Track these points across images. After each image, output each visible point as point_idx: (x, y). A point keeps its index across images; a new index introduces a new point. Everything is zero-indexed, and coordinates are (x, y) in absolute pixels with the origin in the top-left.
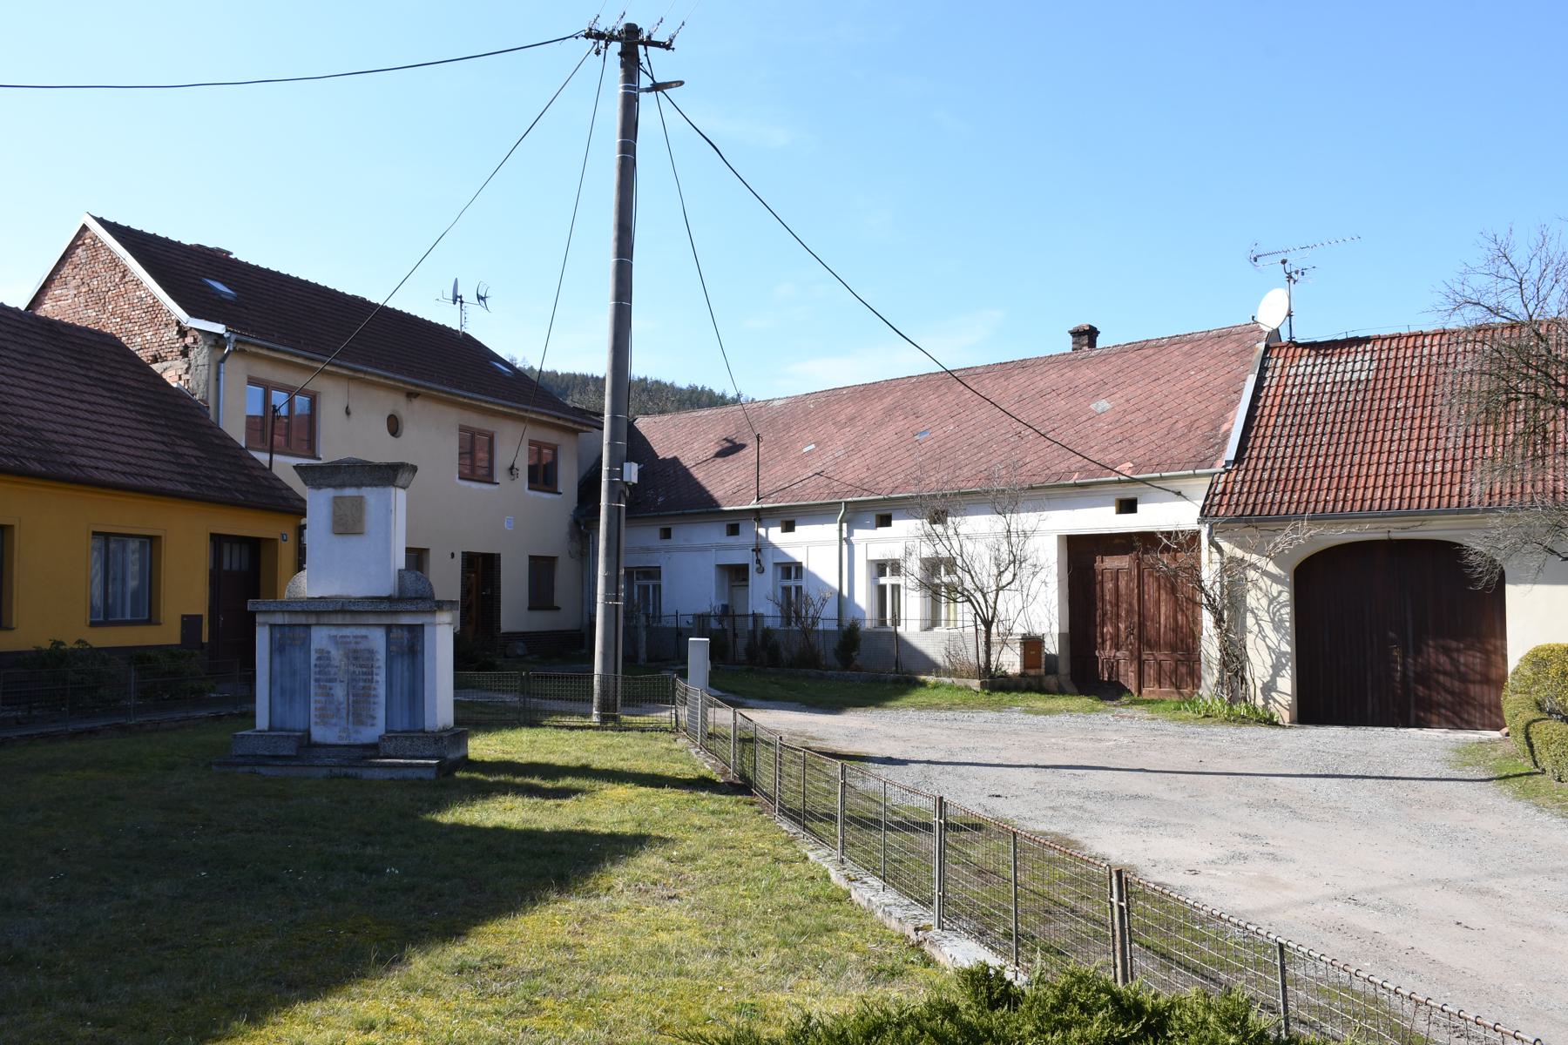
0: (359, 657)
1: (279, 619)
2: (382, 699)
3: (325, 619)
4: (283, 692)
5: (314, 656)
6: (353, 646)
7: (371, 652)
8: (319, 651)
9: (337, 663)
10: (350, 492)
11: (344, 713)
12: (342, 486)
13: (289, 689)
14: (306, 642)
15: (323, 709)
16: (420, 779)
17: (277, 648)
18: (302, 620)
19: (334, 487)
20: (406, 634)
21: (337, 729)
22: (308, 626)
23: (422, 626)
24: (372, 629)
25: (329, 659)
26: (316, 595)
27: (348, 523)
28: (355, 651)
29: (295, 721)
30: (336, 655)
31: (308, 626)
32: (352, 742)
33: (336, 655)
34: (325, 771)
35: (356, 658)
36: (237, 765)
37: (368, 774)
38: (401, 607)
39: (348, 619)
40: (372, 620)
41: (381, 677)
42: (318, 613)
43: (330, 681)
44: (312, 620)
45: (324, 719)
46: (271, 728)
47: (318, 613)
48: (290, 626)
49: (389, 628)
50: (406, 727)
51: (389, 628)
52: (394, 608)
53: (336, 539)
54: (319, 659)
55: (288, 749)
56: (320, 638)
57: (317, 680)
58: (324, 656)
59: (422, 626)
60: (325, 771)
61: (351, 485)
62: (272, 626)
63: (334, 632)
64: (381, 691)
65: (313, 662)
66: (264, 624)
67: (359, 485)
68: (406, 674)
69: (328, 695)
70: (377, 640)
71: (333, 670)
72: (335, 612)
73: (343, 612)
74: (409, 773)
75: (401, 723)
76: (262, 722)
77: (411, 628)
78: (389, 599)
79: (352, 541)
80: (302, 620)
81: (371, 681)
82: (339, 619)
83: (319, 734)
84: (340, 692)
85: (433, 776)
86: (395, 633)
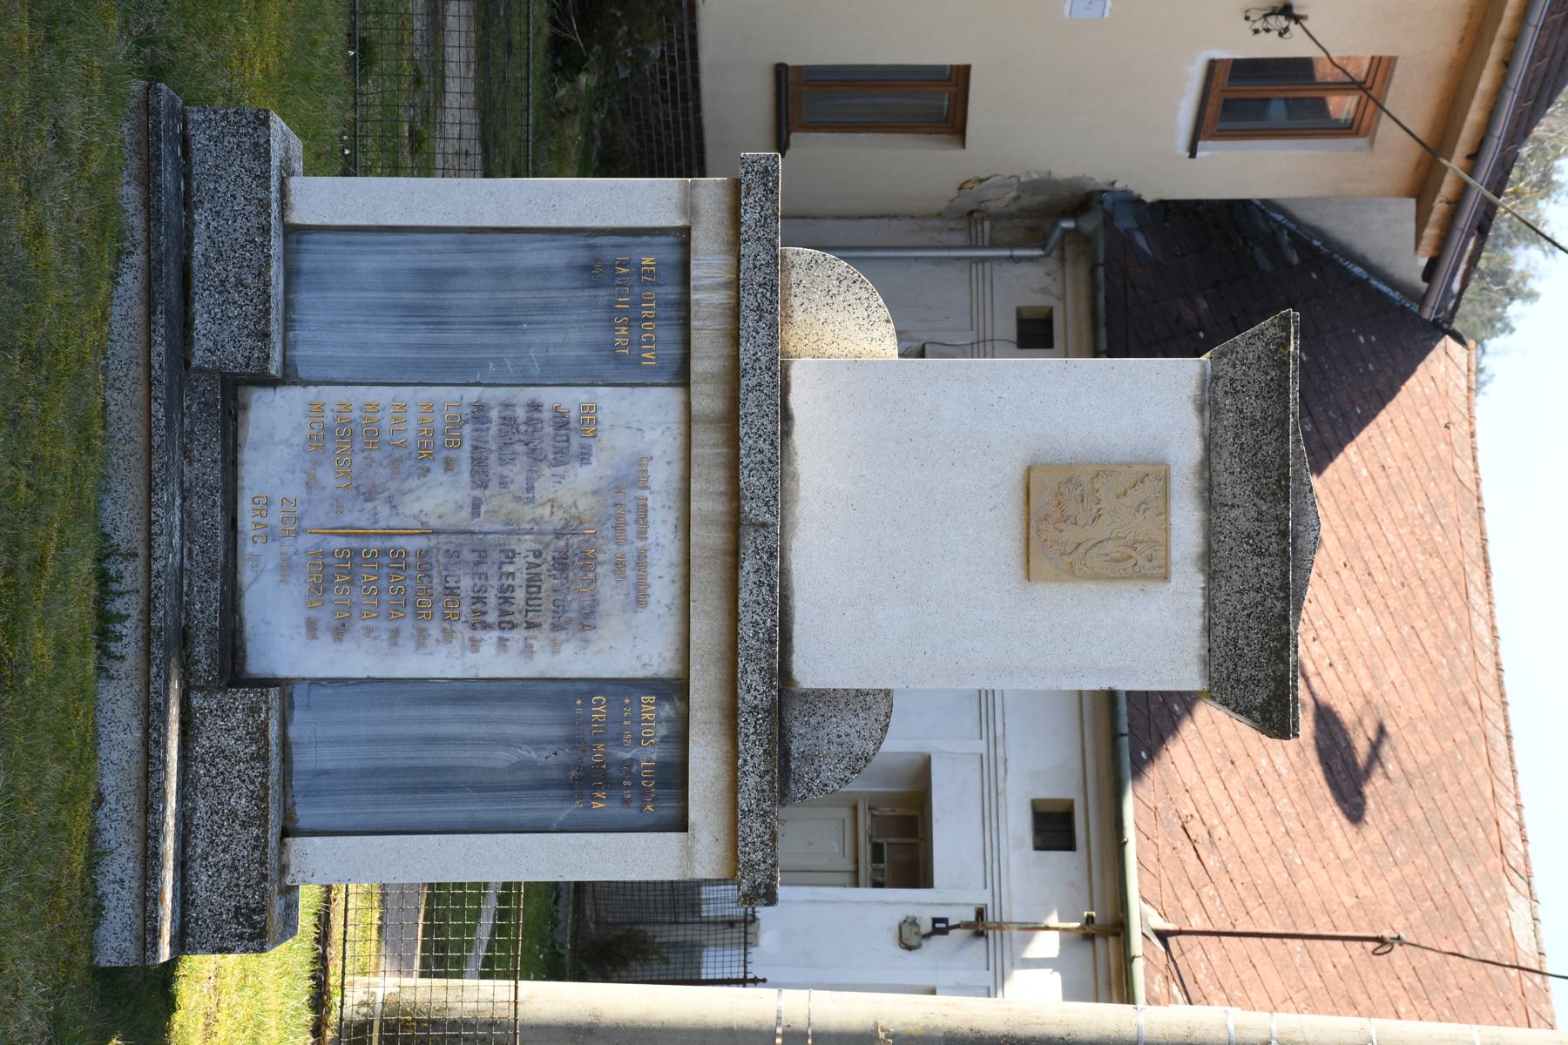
0: (564, 578)
1: (709, 265)
2: (410, 664)
3: (708, 446)
4: (434, 278)
5: (570, 399)
6: (608, 552)
7: (587, 621)
8: (589, 419)
9: (545, 486)
10: (1186, 525)
11: (357, 516)
12: (1210, 497)
13: (437, 285)
14: (621, 370)
15: (373, 437)
16: (98, 911)
17: (599, 259)
18: (707, 360)
19: (1206, 464)
20: (650, 755)
21: (295, 490)
22: (682, 377)
23: (681, 825)
24: (671, 624)
25: (561, 457)
26: (798, 400)
27: (1065, 519)
28: (588, 561)
29: (322, 330)
30: (574, 488)
31: (682, 377)
32: (248, 549)
33: (574, 488)
34: (127, 533)
35: (562, 563)
36: (148, 181)
37: (118, 704)
38: (754, 752)
39: (708, 538)
40: (706, 630)
41: (492, 659)
42: (731, 419)
43: (479, 463)
44: (707, 399)
45: (333, 438)
46: (294, 232)
47: (731, 419)
48: (684, 305)
49: (676, 688)
50: (304, 760)
51: (676, 688)
52: (747, 726)
53: (1012, 474)
54: (561, 422)
55: (215, 334)
56: (639, 424)
57: (480, 409)
58: (570, 439)
59: (681, 825)
60: (127, 533)
61: (1210, 532)
62: (683, 237)
63: (663, 476)
64: (442, 661)
65: (551, 397)
66: (690, 209)
67: (1210, 562)
68: (503, 757)
69: (427, 454)
70: (630, 643)
71: (517, 473)
72: (735, 494)
73: (736, 523)
74: (121, 865)
75: (319, 742)
76: (321, 199)
77: (675, 776)
78: (784, 674)
79: (996, 532)
80: (707, 360)
81: (479, 624)
82: (708, 503)
83: (275, 419)
84: (437, 499)
85: (108, 957)
86: (653, 714)
